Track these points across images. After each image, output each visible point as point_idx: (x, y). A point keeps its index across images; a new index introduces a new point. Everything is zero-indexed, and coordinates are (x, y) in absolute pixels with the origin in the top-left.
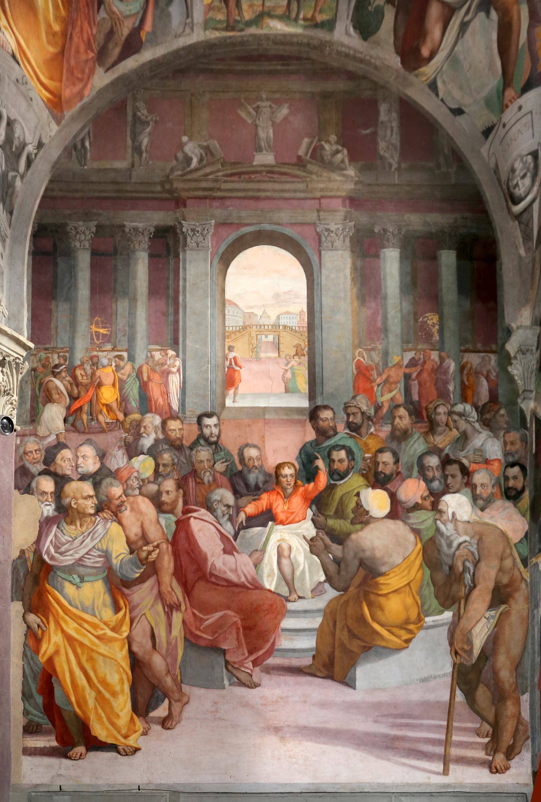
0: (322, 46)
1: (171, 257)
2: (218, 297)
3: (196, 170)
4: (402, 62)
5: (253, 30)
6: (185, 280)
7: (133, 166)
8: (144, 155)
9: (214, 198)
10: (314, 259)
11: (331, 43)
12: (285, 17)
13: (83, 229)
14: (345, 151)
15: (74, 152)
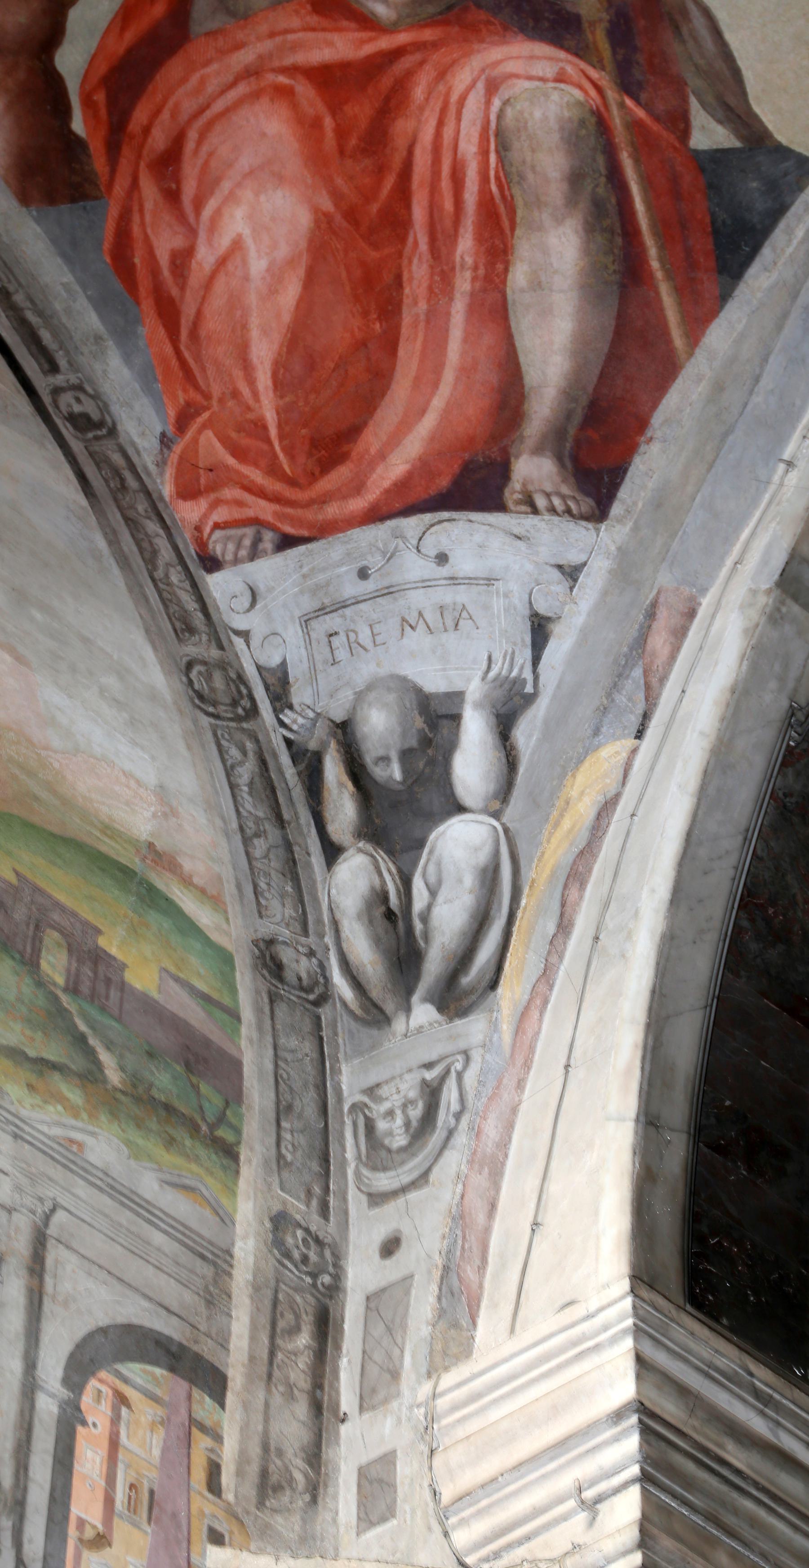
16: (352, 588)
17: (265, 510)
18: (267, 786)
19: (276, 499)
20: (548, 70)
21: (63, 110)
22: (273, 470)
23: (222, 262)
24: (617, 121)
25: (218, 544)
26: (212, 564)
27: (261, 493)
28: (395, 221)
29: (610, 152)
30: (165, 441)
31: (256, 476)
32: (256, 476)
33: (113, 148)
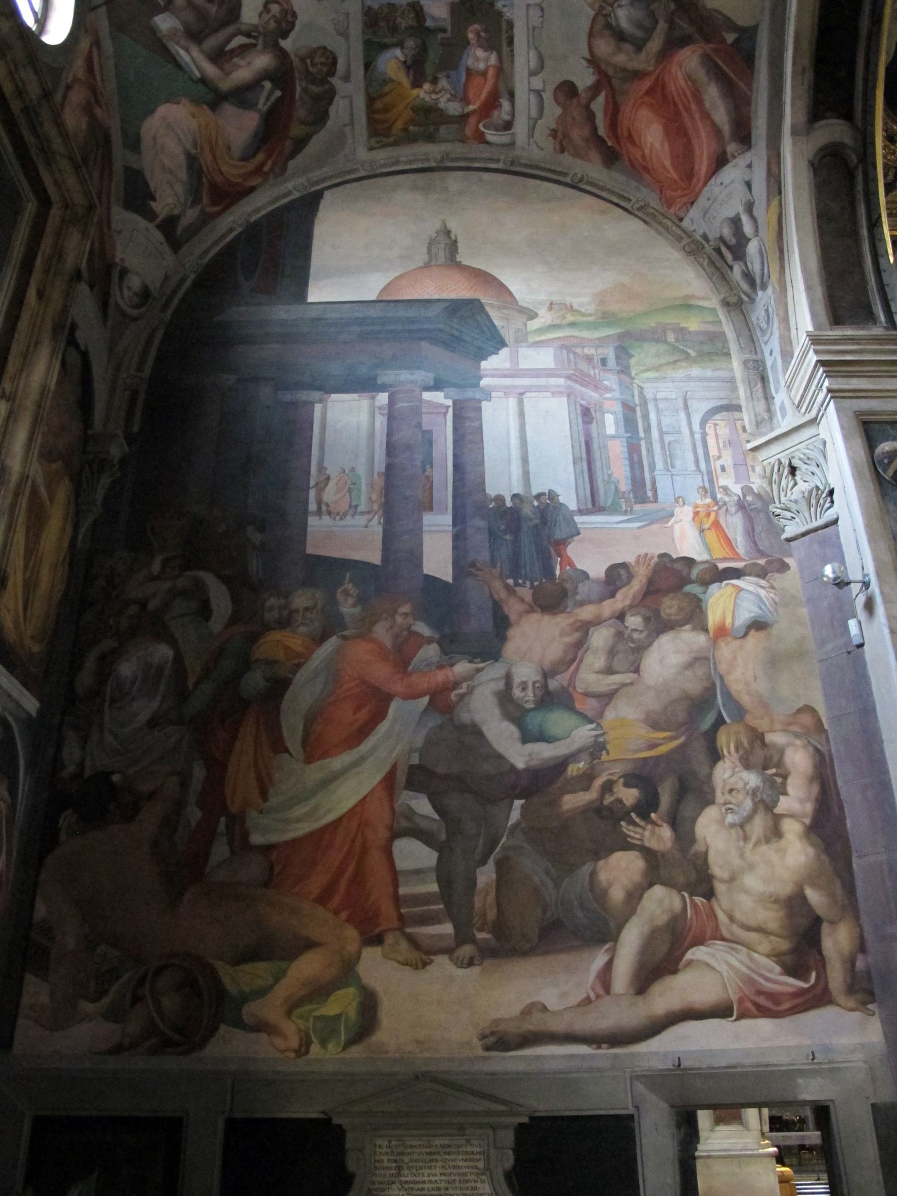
16: (708, 204)
17: (685, 199)
18: (712, 263)
19: (686, 195)
20: (689, 53)
22: (684, 189)
23: (651, 150)
24: (709, 52)
25: (681, 214)
26: (681, 220)
27: (683, 196)
28: (677, 113)
30: (660, 199)
31: (679, 193)
32: (679, 193)
33: (618, 142)
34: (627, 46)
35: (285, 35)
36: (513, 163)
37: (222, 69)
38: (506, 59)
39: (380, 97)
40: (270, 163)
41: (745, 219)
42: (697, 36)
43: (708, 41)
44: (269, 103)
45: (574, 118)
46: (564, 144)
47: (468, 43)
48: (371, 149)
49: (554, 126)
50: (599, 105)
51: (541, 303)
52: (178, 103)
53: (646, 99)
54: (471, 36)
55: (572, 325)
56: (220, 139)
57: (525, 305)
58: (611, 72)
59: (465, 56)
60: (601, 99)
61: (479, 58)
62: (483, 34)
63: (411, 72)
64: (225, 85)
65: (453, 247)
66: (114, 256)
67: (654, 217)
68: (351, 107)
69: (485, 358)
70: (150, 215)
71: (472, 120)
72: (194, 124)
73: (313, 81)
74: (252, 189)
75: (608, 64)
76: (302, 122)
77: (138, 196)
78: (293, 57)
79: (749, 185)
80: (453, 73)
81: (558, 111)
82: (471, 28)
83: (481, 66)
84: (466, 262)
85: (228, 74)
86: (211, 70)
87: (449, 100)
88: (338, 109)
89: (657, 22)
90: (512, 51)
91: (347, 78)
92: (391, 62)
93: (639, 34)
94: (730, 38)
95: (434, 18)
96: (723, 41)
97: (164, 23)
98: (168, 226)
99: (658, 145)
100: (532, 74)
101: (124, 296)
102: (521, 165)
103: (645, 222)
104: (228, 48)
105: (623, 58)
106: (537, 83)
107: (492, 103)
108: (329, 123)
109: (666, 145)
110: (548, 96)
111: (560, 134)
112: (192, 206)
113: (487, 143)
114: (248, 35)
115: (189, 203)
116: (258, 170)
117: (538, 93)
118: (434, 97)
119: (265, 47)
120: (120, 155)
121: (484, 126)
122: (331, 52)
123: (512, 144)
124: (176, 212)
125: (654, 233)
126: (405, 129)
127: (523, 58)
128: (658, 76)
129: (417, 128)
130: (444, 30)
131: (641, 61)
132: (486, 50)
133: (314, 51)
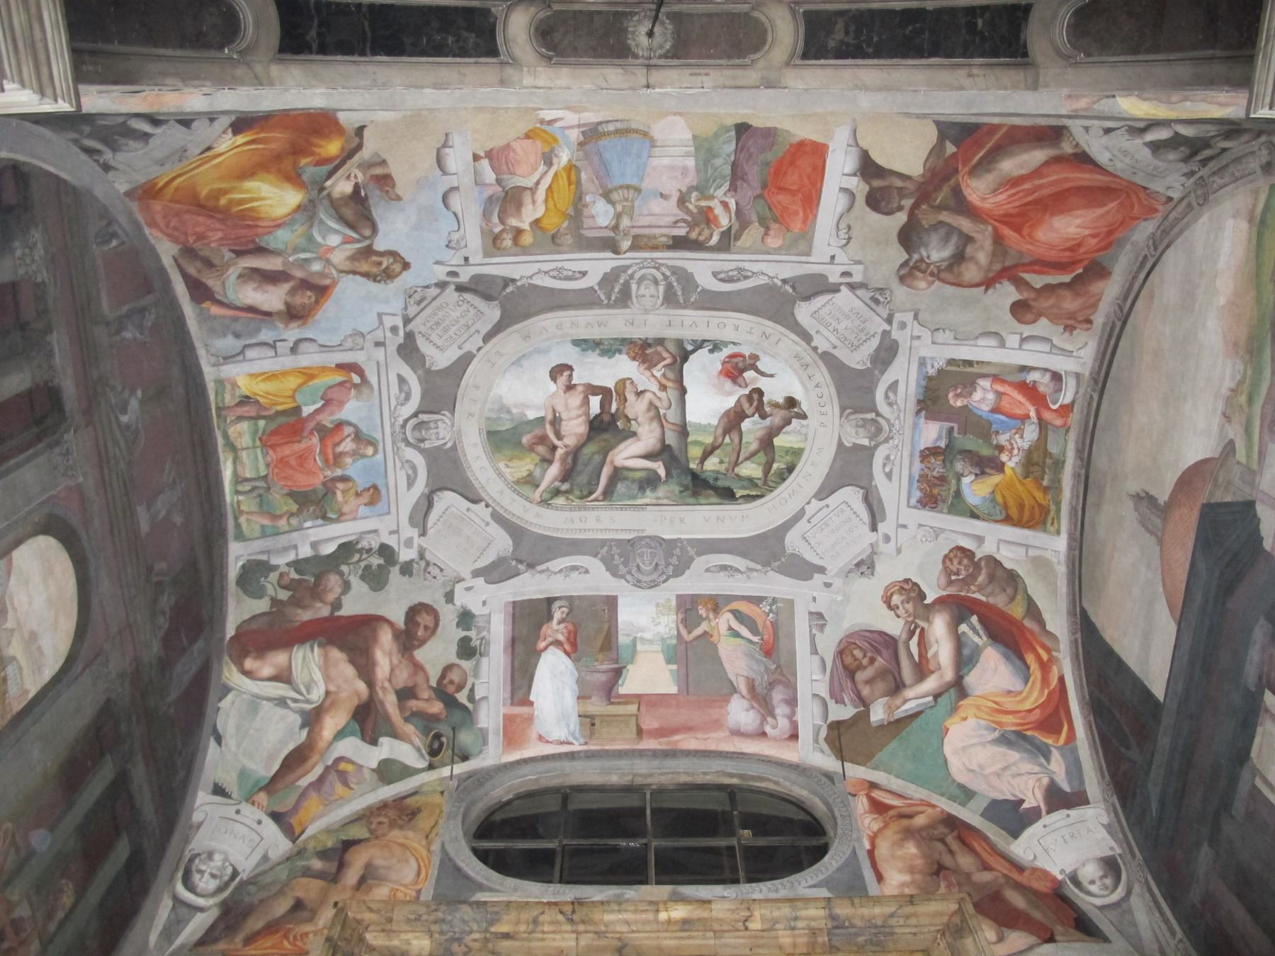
0: (223, 533)
1: (35, 430)
2: (11, 537)
3: (119, 425)
4: (231, 638)
5: (220, 441)
6: (18, 466)
7: (108, 324)
8: (118, 338)
9: (101, 467)
10: (78, 667)
11: (226, 543)
12: (238, 480)
13: (37, 258)
14: (166, 626)
15: (104, 223)
17: (1142, 196)
18: (1219, 172)
21: (1080, 275)
22: (1128, 196)
24: (967, 169)
25: (1164, 199)
26: (1170, 199)
28: (1036, 202)
29: (975, 167)
30: (1146, 220)
31: (1135, 200)
32: (1135, 200)
33: (1081, 261)
34: (969, 250)
35: (922, 596)
36: (1096, 382)
37: (933, 672)
38: (985, 370)
39: (1006, 506)
40: (1041, 651)
41: (1151, 137)
42: (952, 182)
43: (956, 171)
44: (981, 632)
45: (1052, 307)
46: (1081, 318)
47: (966, 406)
48: (1058, 532)
49: (1061, 328)
50: (1037, 281)
51: (1222, 428)
52: (948, 730)
53: (1025, 231)
54: (959, 403)
55: (1250, 400)
56: (997, 699)
57: (1220, 449)
58: (998, 267)
59: (980, 413)
60: (1027, 277)
61: (983, 398)
62: (959, 391)
63: (988, 470)
64: (949, 675)
65: (1151, 499)
66: (1054, 879)
67: (1165, 232)
68: (1009, 542)
69: (1260, 540)
70: (1034, 815)
71: (1047, 416)
72: (972, 722)
73: (972, 577)
74: (1061, 680)
75: (989, 270)
76: (1012, 599)
77: (1014, 817)
78: (945, 593)
79: (1108, 131)
80: (994, 427)
81: (1044, 321)
82: (952, 402)
83: (991, 396)
84: (1166, 497)
85: (939, 668)
86: (931, 684)
87: (1022, 437)
88: (1009, 558)
89: (941, 223)
90: (978, 362)
91: (980, 540)
92: (975, 490)
93: (954, 239)
94: (950, 149)
95: (939, 438)
96: (954, 155)
97: (878, 714)
98: (1058, 799)
99: (1078, 221)
100: (1002, 344)
101: (1096, 896)
102: (1098, 373)
103: (1168, 246)
104: (916, 658)
105: (982, 255)
106: (1013, 341)
107: (1030, 391)
108: (1020, 572)
109: (1079, 212)
110: (1027, 330)
111: (1070, 322)
112: (1048, 760)
113: (1073, 403)
114: (912, 634)
115: (1042, 760)
116: (1045, 667)
117: (1023, 340)
118: (1016, 452)
119: (927, 620)
120: (970, 815)
121: (1055, 403)
122: (951, 551)
123: (1078, 376)
124: (1046, 781)
125: (1180, 240)
126: (1046, 490)
127: (985, 352)
128: (999, 221)
129: (1046, 477)
130: (951, 431)
131: (983, 236)
132: (975, 390)
133: (945, 568)
